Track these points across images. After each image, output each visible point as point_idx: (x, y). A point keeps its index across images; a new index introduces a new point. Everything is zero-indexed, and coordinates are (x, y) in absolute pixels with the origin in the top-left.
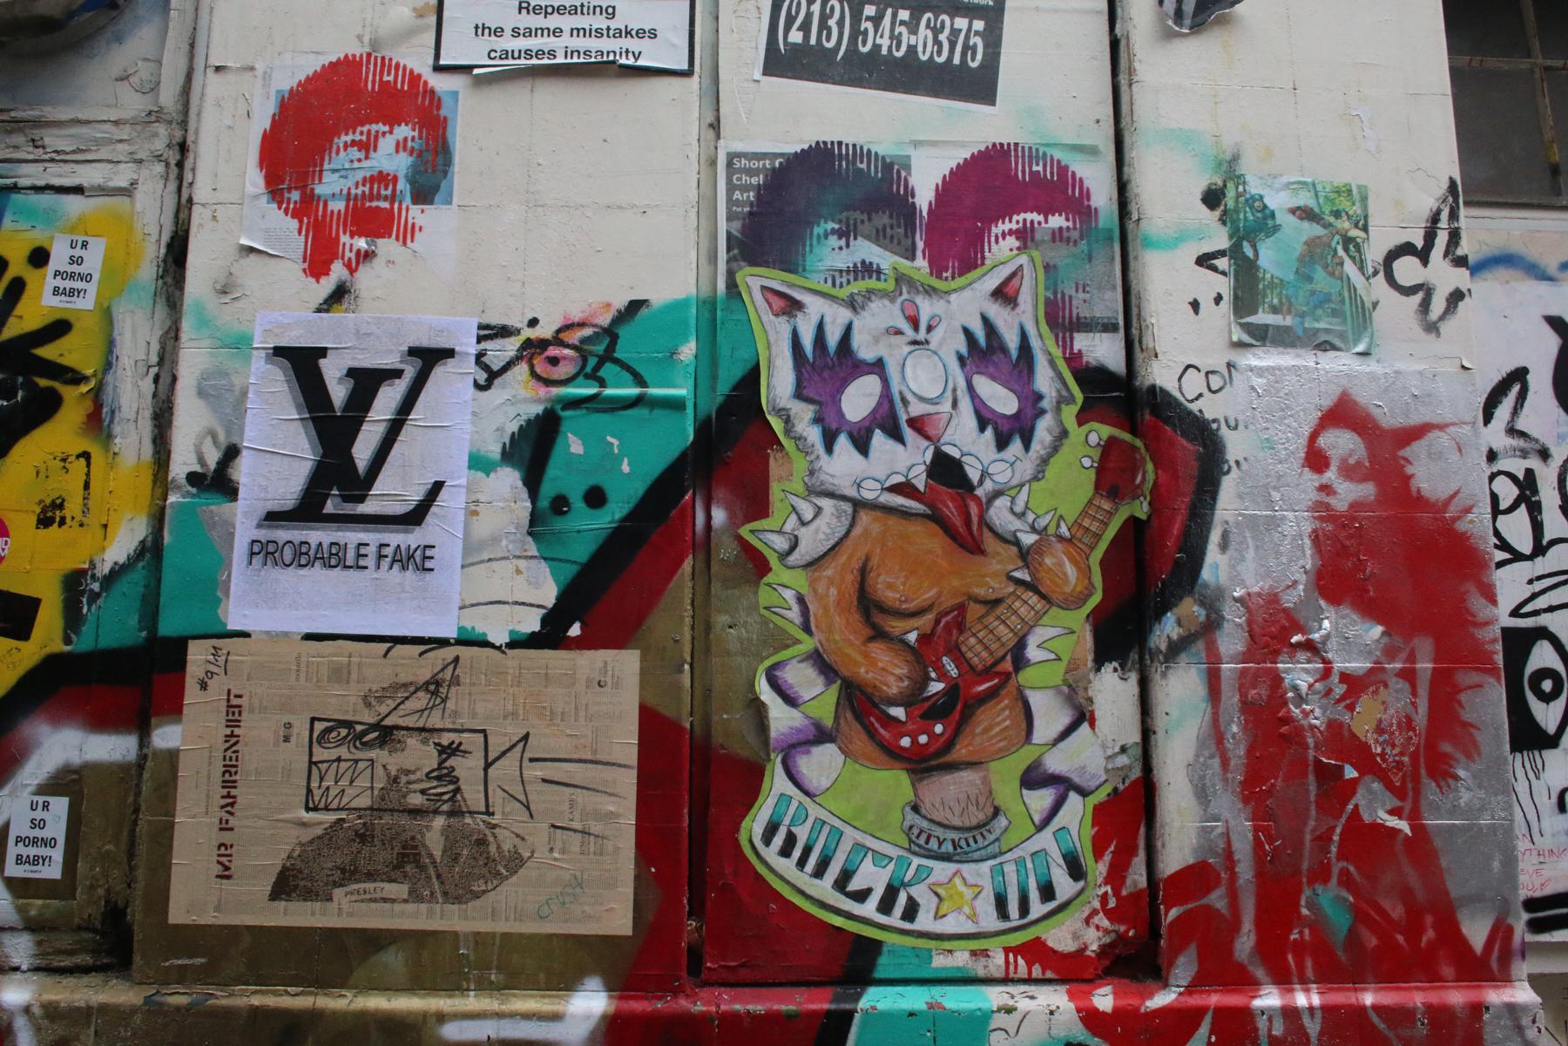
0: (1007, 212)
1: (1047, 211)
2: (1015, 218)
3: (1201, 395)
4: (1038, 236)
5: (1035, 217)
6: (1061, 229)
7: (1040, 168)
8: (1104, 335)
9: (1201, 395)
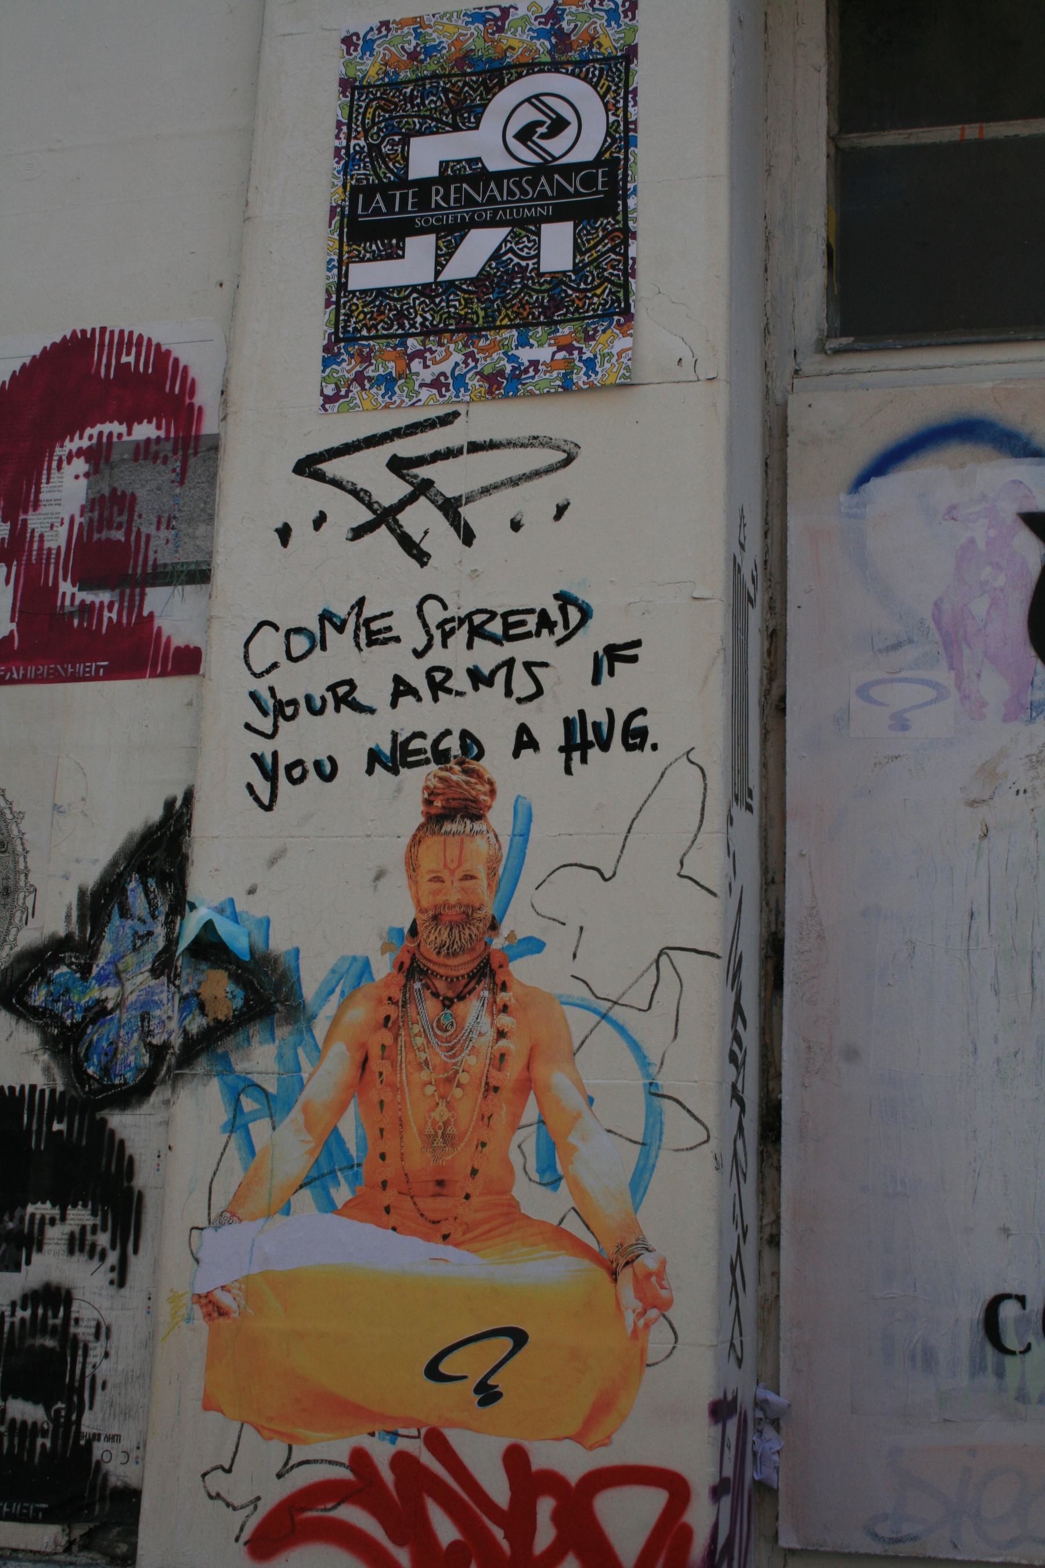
0: (77, 427)
1: (130, 419)
2: (88, 431)
3: (275, 666)
4: (115, 457)
5: (116, 428)
6: (148, 440)
7: (131, 359)
8: (188, 588)
9: (275, 666)
